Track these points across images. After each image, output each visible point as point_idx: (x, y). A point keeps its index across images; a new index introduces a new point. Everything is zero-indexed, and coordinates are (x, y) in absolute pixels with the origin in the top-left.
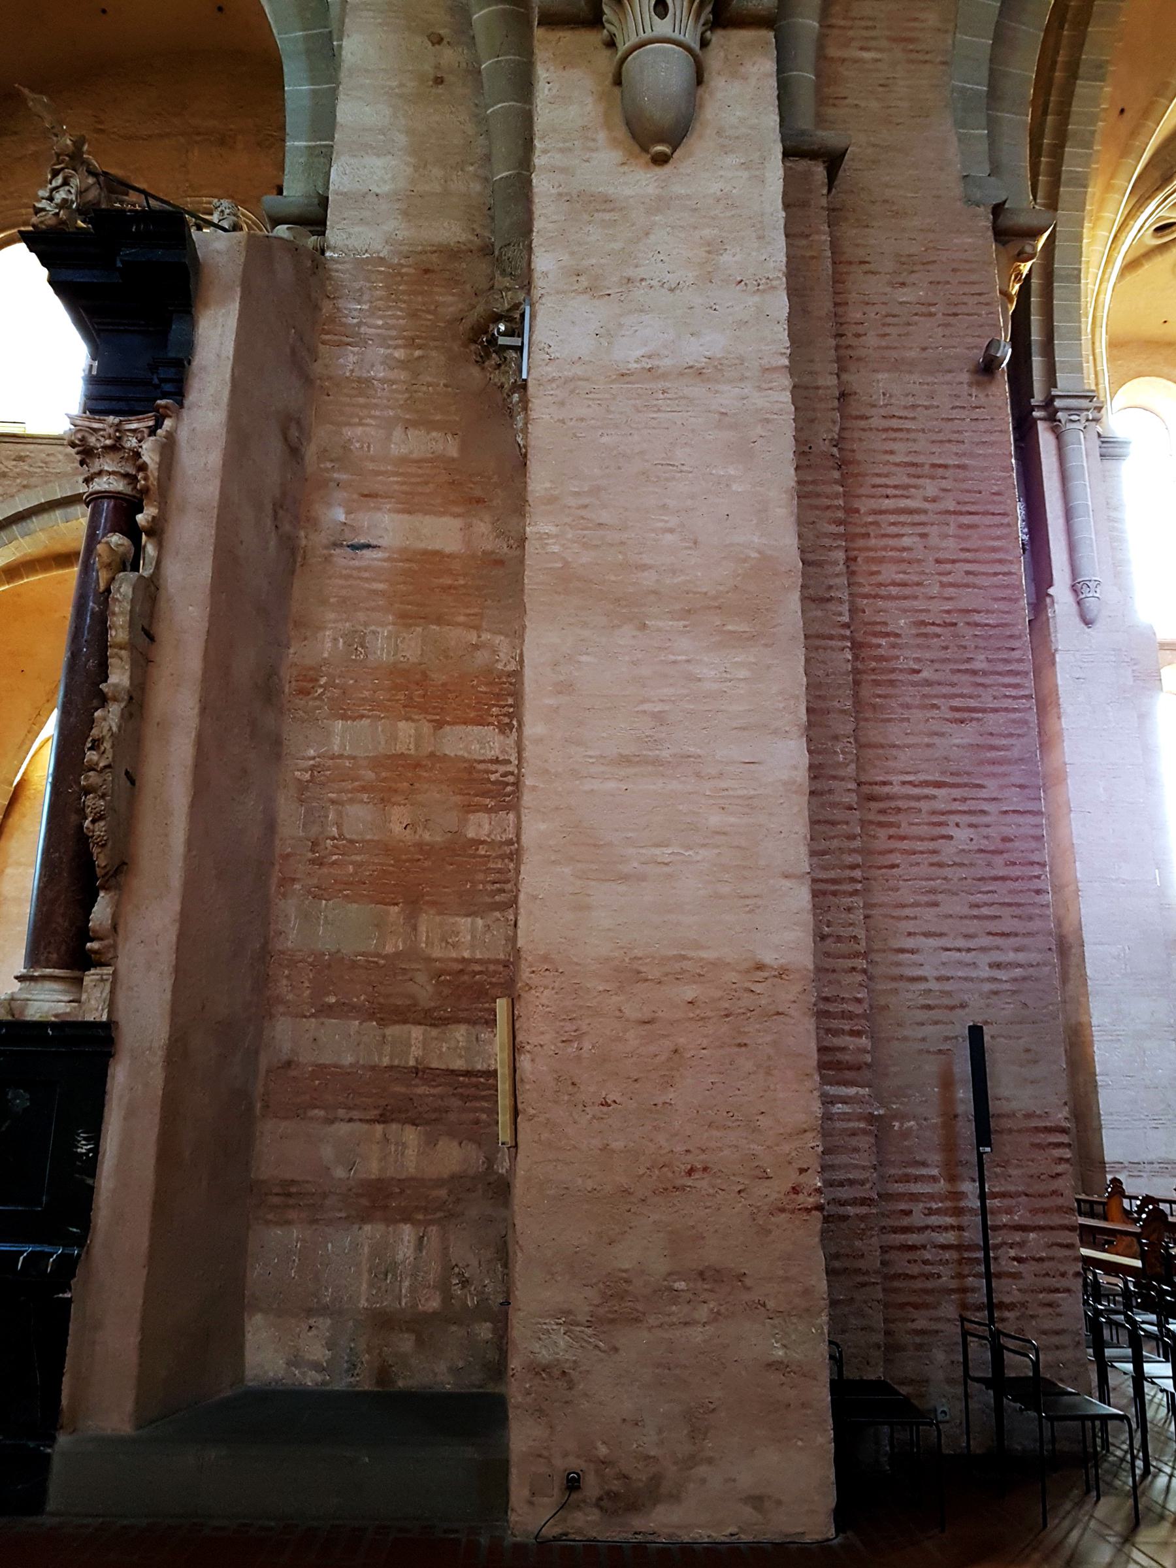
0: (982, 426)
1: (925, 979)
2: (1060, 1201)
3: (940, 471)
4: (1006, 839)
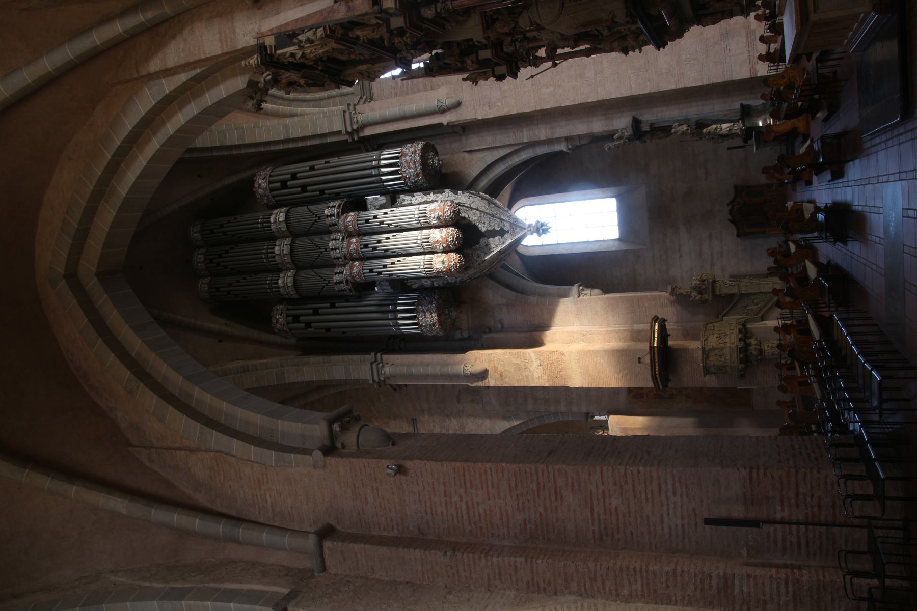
1: (683, 526)
4: (615, 483)
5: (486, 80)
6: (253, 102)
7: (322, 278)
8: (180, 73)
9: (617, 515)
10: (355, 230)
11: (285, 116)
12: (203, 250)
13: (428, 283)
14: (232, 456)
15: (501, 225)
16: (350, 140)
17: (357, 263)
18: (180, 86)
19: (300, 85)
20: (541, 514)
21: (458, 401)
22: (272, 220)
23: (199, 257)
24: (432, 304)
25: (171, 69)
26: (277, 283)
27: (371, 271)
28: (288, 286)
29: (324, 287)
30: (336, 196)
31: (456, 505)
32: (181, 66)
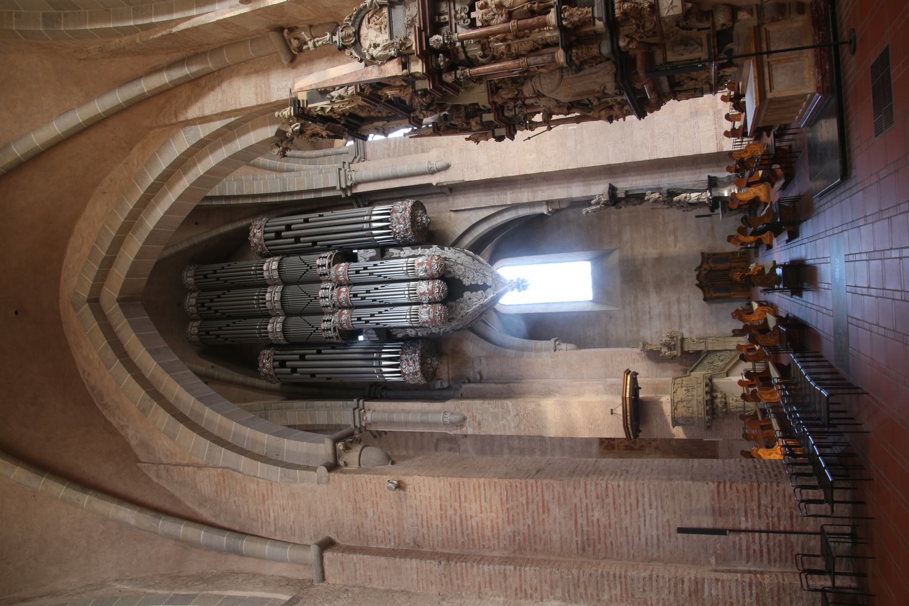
0: (422, 488)
1: (658, 536)
2: (748, 490)
3: (443, 507)
4: (597, 497)
5: (487, 140)
6: (278, 149)
7: (310, 325)
8: (216, 121)
9: (599, 526)
10: (345, 280)
11: (281, 171)
12: (195, 295)
13: (411, 333)
14: (239, 472)
15: (484, 280)
16: (343, 196)
17: (345, 311)
18: (214, 132)
19: (322, 137)
20: (529, 526)
21: (436, 449)
22: (265, 268)
23: (191, 300)
24: (415, 354)
25: (208, 116)
26: (266, 329)
27: (359, 319)
28: (277, 332)
29: (312, 333)
30: (328, 248)
31: (451, 518)
32: (216, 115)
